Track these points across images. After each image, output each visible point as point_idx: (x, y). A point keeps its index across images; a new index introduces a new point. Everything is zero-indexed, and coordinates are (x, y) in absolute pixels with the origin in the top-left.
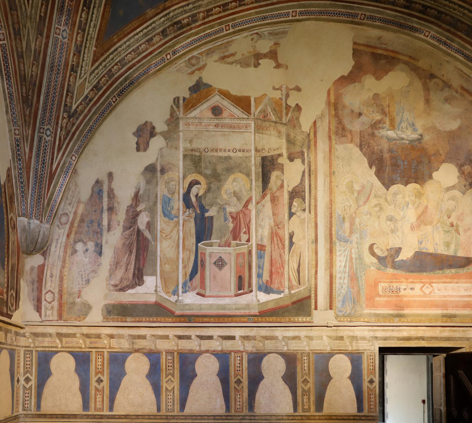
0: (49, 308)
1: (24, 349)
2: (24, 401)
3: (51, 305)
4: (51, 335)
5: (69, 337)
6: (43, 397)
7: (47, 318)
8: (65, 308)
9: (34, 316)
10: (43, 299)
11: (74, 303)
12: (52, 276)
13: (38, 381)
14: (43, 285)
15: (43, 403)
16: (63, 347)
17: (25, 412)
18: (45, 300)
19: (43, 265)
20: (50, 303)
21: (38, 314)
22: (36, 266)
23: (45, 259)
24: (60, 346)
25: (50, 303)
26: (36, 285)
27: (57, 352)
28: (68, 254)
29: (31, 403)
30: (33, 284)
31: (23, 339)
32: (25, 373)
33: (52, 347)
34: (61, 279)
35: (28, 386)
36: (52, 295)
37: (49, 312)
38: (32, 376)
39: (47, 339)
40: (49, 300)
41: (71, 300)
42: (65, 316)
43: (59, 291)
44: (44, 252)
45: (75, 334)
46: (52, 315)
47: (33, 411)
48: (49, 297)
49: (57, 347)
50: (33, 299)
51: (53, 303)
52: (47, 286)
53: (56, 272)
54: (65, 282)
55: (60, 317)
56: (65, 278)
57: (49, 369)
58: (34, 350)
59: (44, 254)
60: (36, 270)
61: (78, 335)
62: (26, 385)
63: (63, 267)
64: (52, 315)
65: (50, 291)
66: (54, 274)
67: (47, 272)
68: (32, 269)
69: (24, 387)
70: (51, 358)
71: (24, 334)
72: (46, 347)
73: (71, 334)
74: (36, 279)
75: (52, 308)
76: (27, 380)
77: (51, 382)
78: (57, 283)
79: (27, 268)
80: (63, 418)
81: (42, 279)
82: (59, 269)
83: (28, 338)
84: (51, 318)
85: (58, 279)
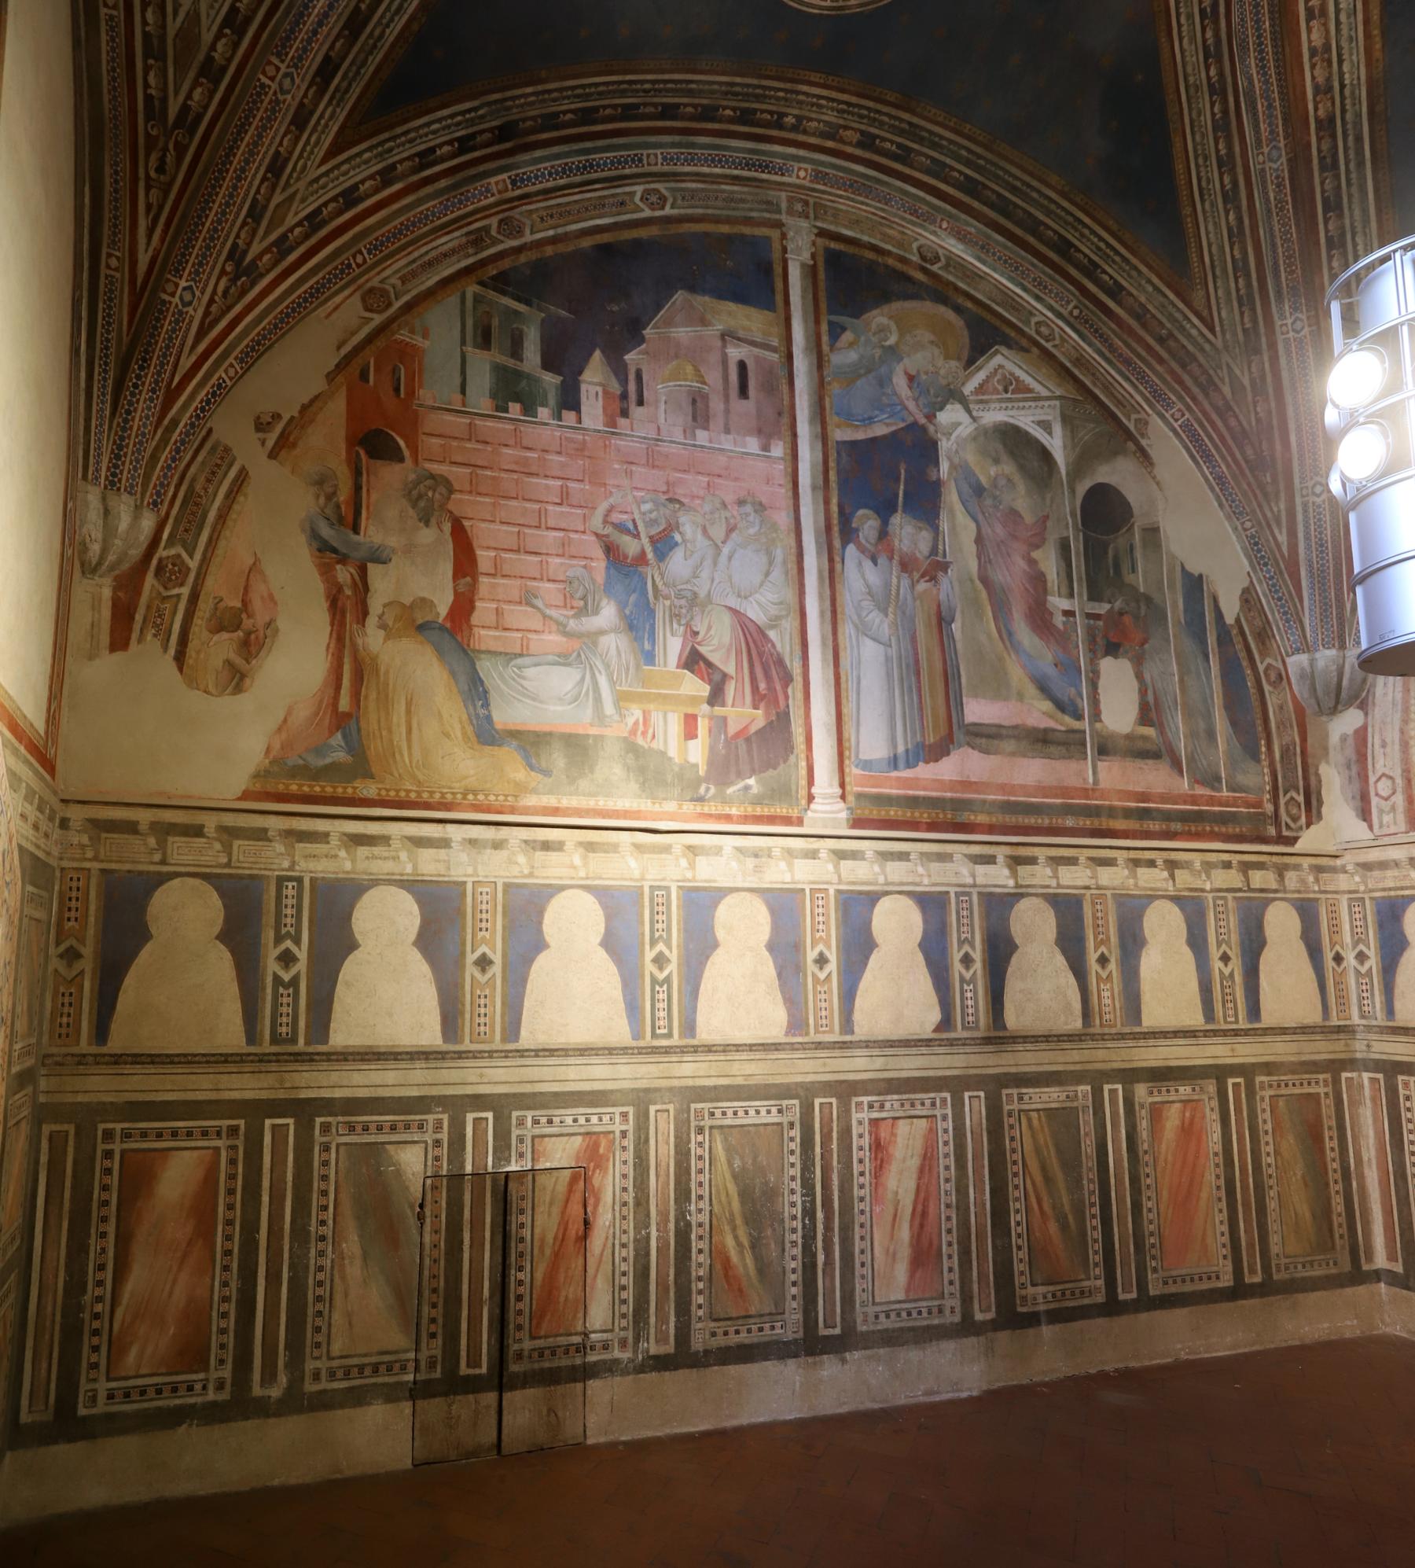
0: (1387, 809)
1: (1346, 896)
2: (1361, 999)
4: (1397, 864)
6: (1397, 991)
7: (1385, 831)
9: (1358, 830)
10: (1372, 793)
12: (1384, 745)
13: (1383, 958)
15: (1398, 1005)
17: (1364, 1022)
18: (1377, 794)
19: (1364, 728)
20: (1386, 799)
21: (1365, 825)
23: (1366, 714)
25: (1386, 799)
26: (1354, 769)
29: (1373, 1003)
30: (1349, 767)
32: (1356, 944)
33: (1402, 888)
34: (1405, 746)
35: (1363, 970)
36: (1389, 782)
37: (1386, 819)
39: (1389, 873)
40: (1384, 794)
43: (1404, 771)
44: (1362, 702)
46: (1395, 823)
47: (1380, 1019)
48: (1384, 787)
51: (1393, 799)
52: (1378, 766)
53: (1393, 736)
58: (1366, 896)
59: (1363, 706)
60: (1350, 741)
62: (1359, 967)
63: (1405, 721)
65: (1384, 775)
66: (1388, 740)
67: (1374, 740)
68: (1344, 739)
69: (1358, 972)
70: (1404, 911)
71: (1344, 866)
72: (1390, 889)
74: (1354, 757)
75: (1393, 809)
76: (1361, 957)
78: (1397, 755)
79: (1334, 738)
82: (1397, 728)
83: (1352, 875)
84: (1393, 830)
85: (1397, 747)
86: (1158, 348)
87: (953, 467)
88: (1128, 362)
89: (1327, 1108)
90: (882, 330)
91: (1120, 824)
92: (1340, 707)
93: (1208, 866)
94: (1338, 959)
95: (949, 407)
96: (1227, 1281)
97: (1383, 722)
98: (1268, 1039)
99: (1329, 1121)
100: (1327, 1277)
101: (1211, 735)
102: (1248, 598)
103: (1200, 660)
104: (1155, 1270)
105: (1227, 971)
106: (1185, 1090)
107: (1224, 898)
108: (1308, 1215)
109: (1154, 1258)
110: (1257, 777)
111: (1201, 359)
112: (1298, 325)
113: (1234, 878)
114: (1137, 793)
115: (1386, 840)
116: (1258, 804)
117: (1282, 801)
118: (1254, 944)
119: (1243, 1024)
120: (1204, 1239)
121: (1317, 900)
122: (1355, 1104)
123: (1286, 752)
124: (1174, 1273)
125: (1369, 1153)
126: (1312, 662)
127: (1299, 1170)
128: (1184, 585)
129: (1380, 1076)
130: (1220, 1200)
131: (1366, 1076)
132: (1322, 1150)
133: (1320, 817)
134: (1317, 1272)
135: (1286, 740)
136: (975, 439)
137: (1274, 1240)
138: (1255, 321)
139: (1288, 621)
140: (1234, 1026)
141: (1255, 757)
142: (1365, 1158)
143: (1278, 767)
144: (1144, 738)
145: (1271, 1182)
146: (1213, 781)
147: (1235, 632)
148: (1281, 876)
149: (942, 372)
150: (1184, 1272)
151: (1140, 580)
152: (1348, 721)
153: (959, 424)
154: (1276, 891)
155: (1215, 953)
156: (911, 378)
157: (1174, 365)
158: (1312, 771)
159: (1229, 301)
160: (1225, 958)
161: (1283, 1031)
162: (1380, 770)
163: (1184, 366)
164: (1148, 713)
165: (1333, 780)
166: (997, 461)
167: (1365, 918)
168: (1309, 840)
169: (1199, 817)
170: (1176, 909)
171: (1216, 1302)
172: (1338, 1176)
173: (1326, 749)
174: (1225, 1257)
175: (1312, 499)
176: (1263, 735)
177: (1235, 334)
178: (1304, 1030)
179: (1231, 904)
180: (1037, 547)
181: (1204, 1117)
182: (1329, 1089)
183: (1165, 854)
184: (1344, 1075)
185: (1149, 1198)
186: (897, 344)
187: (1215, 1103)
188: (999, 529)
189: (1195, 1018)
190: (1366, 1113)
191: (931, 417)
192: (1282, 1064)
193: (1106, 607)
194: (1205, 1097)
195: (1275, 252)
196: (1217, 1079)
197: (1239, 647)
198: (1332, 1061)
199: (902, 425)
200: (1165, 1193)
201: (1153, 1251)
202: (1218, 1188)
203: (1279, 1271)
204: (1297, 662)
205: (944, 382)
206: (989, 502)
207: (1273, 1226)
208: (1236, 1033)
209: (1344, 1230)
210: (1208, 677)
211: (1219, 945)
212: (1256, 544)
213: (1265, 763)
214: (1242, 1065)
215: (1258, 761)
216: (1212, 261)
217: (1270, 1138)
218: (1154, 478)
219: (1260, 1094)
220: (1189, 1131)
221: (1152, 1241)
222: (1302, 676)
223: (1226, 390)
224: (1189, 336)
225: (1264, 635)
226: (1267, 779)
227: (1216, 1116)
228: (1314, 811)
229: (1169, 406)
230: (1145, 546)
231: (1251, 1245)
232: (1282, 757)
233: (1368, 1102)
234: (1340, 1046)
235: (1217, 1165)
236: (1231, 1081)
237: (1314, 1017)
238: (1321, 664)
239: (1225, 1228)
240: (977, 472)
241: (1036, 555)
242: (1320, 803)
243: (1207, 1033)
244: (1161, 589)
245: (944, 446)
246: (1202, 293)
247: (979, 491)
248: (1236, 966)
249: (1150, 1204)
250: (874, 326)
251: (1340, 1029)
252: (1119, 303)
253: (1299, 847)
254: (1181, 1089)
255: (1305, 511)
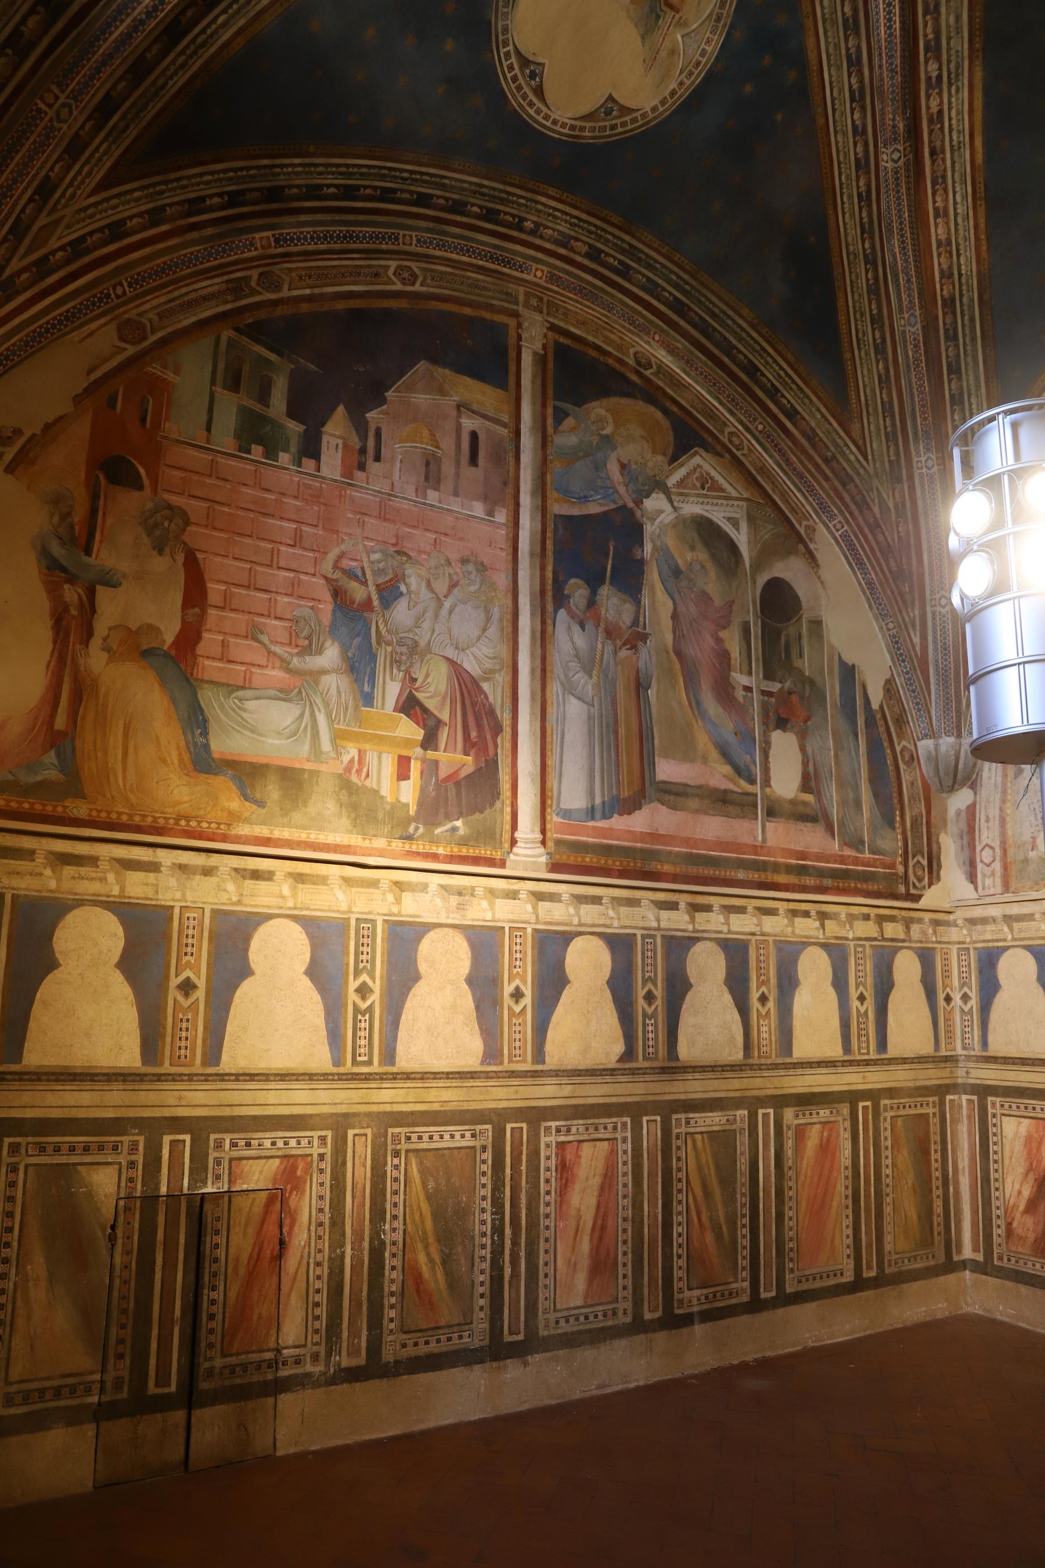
0: (989, 874)
1: (957, 946)
2: (964, 1033)
3: (991, 869)
4: (994, 920)
5: (1023, 921)
6: (991, 1027)
8: (1013, 872)
10: (978, 860)
11: (1026, 860)
12: (988, 820)
13: (981, 999)
14: (977, 838)
15: (991, 1038)
16: (1014, 939)
17: (965, 1053)
21: (971, 886)
22: (963, 808)
24: (1010, 937)
25: (988, 865)
26: (966, 839)
27: (1007, 948)
28: (1009, 779)
29: (973, 1036)
30: (962, 838)
31: (954, 929)
33: (997, 941)
35: (966, 1009)
36: (991, 851)
37: (988, 882)
38: (971, 991)
39: (989, 928)
40: (987, 861)
41: (1021, 856)
42: (1013, 885)
44: (972, 783)
45: (1032, 915)
46: (994, 886)
48: (986, 855)
49: (1005, 940)
50: (964, 863)
51: (993, 865)
52: (983, 837)
53: (994, 813)
54: (1009, 826)
55: (1006, 887)
56: (1008, 819)
57: (997, 980)
59: (973, 787)
60: (963, 815)
61: (1037, 916)
62: (963, 1006)
63: (1004, 801)
64: (994, 886)
66: (991, 816)
67: (981, 816)
68: (958, 813)
69: (962, 1010)
70: (998, 959)
71: (955, 921)
72: (989, 941)
73: (1026, 915)
74: (965, 829)
75: (993, 874)
76: (965, 998)
77: (1001, 1002)
78: (997, 829)
79: (951, 813)
80: (1023, 1064)
81: (974, 828)
83: (961, 928)
84: (992, 892)
85: (997, 822)
86: (824, 466)
87: (655, 549)
88: (800, 476)
89: (934, 1124)
90: (600, 420)
91: (782, 879)
92: (956, 787)
93: (851, 918)
94: (948, 999)
95: (654, 495)
96: (849, 1277)
97: (988, 801)
98: (891, 1067)
99: (935, 1137)
100: (927, 1269)
101: (858, 803)
102: (889, 688)
103: (851, 738)
104: (792, 1271)
105: (862, 1010)
106: (824, 1113)
107: (863, 946)
108: (915, 1217)
109: (791, 1260)
110: (891, 842)
111: (857, 481)
112: (930, 463)
113: (868, 929)
114: (797, 852)
115: (987, 900)
116: (893, 866)
117: (911, 864)
118: (884, 986)
119: (873, 1056)
120: (832, 1242)
121: (934, 949)
122: (955, 1121)
123: (915, 822)
124: (807, 1272)
125: (964, 1163)
126: (937, 746)
127: (910, 1179)
128: (840, 673)
129: (975, 1098)
130: (847, 1207)
131: (964, 1097)
132: (928, 1162)
133: (939, 879)
134: (919, 1265)
135: (916, 811)
136: (675, 526)
137: (888, 1238)
138: (897, 454)
139: (919, 710)
140: (866, 1057)
141: (891, 824)
142: (960, 1167)
143: (909, 833)
144: (805, 804)
145: (889, 1190)
146: (857, 843)
147: (879, 716)
148: (908, 928)
149: (650, 464)
150: (814, 1271)
151: (805, 665)
152: (961, 799)
153: (662, 512)
154: (903, 941)
155: (854, 994)
156: (623, 466)
157: (836, 483)
158: (934, 839)
159: (879, 435)
160: (862, 998)
161: (904, 1061)
162: (985, 840)
163: (844, 485)
164: (809, 782)
165: (949, 847)
166: (693, 548)
167: (969, 964)
168: (930, 898)
169: (845, 874)
170: (825, 955)
171: (839, 1295)
172: (940, 1183)
173: (945, 821)
174: (848, 1256)
175: (939, 609)
176: (898, 806)
177: (883, 464)
178: (920, 1060)
179: (868, 951)
180: (725, 628)
181: (838, 1136)
182: (937, 1110)
183: (818, 907)
184: (949, 1097)
185: (791, 1208)
186: (612, 433)
187: (848, 1124)
188: (692, 608)
189: (836, 1051)
190: (963, 1129)
191: (638, 502)
192: (901, 1089)
193: (779, 686)
194: (840, 1119)
195: (913, 400)
196: (851, 1103)
197: (882, 729)
198: (940, 1086)
199: (613, 506)
200: (804, 1203)
201: (792, 1255)
202: (847, 1197)
203: (890, 1265)
204: (925, 746)
205: (651, 474)
206: (684, 583)
207: (888, 1228)
208: (868, 1063)
209: (942, 1228)
210: (858, 755)
211: (857, 987)
212: (897, 643)
213: (899, 831)
214: (871, 1091)
215: (894, 828)
216: (866, 400)
217: (889, 1153)
218: (819, 577)
219: (883, 1114)
220: (826, 1148)
221: (791, 1245)
222: (929, 758)
223: (876, 509)
224: (848, 461)
225: (901, 721)
226: (900, 844)
227: (848, 1135)
228: (935, 873)
229: (832, 517)
230: (810, 636)
231: (869, 1245)
232: (912, 826)
233: (965, 1120)
234: (946, 1073)
235: (847, 1177)
236: (861, 1104)
237: (928, 1049)
238: (943, 749)
239: (850, 1232)
240: (676, 555)
241: (723, 634)
242: (939, 866)
243: (845, 1063)
244: (822, 674)
245: (649, 529)
246: (858, 426)
247: (677, 573)
248: (870, 1005)
249: (791, 1213)
250: (593, 416)
251: (947, 1059)
252: (795, 424)
253: (923, 903)
254: (822, 1112)
255: (934, 619)
